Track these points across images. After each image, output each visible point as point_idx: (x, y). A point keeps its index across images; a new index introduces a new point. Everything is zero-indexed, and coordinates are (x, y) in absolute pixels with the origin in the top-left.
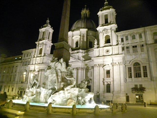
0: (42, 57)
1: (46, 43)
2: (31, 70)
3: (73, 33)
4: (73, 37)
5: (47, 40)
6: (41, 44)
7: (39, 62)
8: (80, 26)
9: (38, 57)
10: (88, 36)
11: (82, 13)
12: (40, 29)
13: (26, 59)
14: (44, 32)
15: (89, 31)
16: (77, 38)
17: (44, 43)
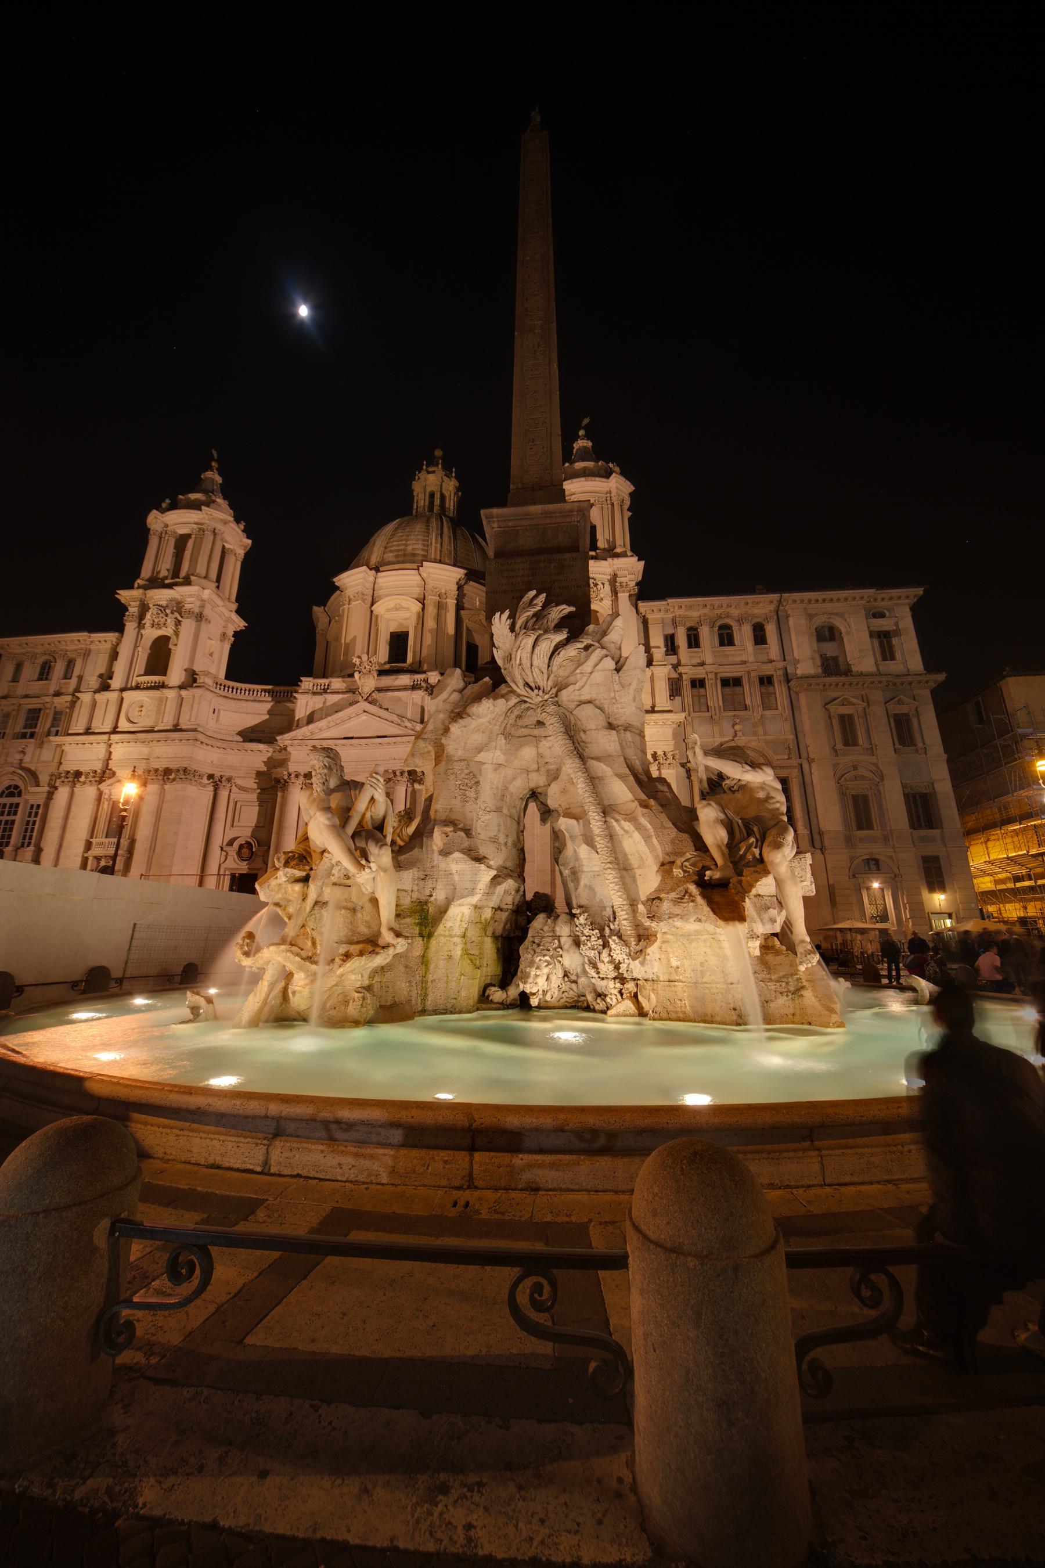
0: (171, 694)
1: (202, 607)
2: (78, 774)
3: (379, 580)
4: (372, 604)
5: (207, 592)
6: (165, 608)
7: (146, 722)
8: (421, 547)
9: (137, 687)
10: (462, 612)
11: (417, 487)
12: (154, 513)
13: (26, 696)
14: (189, 536)
15: (471, 583)
16: (398, 608)
17: (188, 606)
